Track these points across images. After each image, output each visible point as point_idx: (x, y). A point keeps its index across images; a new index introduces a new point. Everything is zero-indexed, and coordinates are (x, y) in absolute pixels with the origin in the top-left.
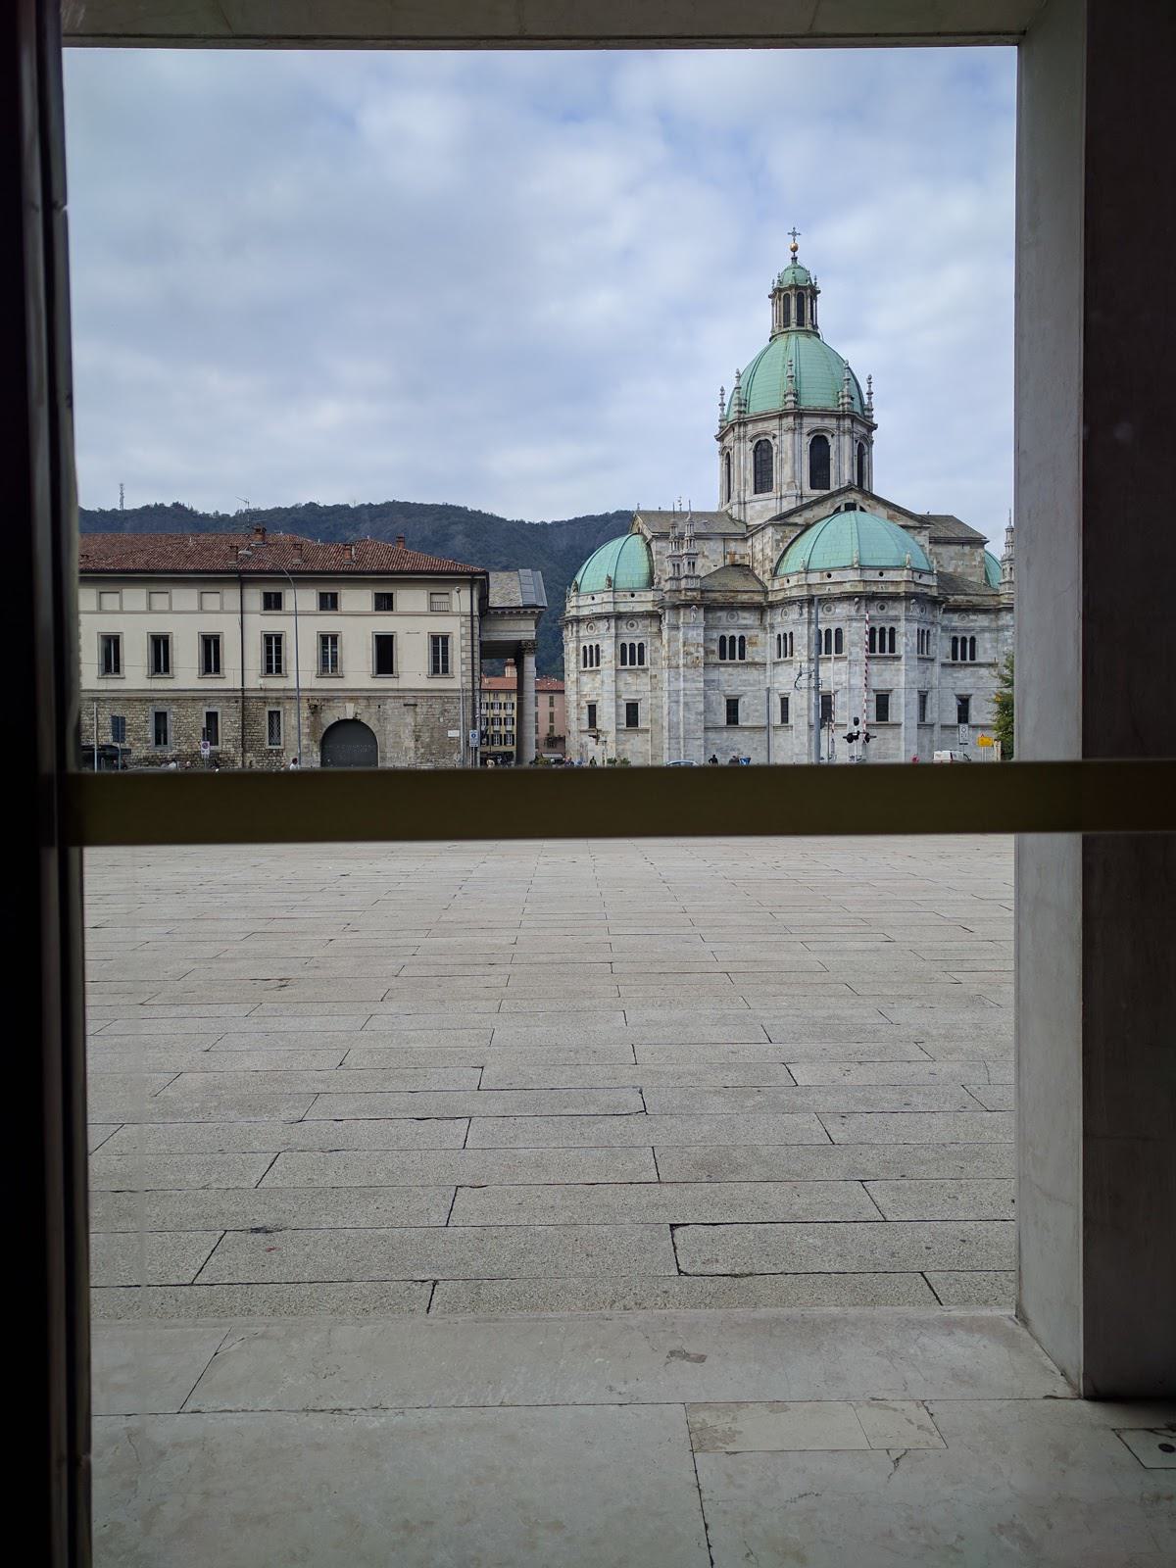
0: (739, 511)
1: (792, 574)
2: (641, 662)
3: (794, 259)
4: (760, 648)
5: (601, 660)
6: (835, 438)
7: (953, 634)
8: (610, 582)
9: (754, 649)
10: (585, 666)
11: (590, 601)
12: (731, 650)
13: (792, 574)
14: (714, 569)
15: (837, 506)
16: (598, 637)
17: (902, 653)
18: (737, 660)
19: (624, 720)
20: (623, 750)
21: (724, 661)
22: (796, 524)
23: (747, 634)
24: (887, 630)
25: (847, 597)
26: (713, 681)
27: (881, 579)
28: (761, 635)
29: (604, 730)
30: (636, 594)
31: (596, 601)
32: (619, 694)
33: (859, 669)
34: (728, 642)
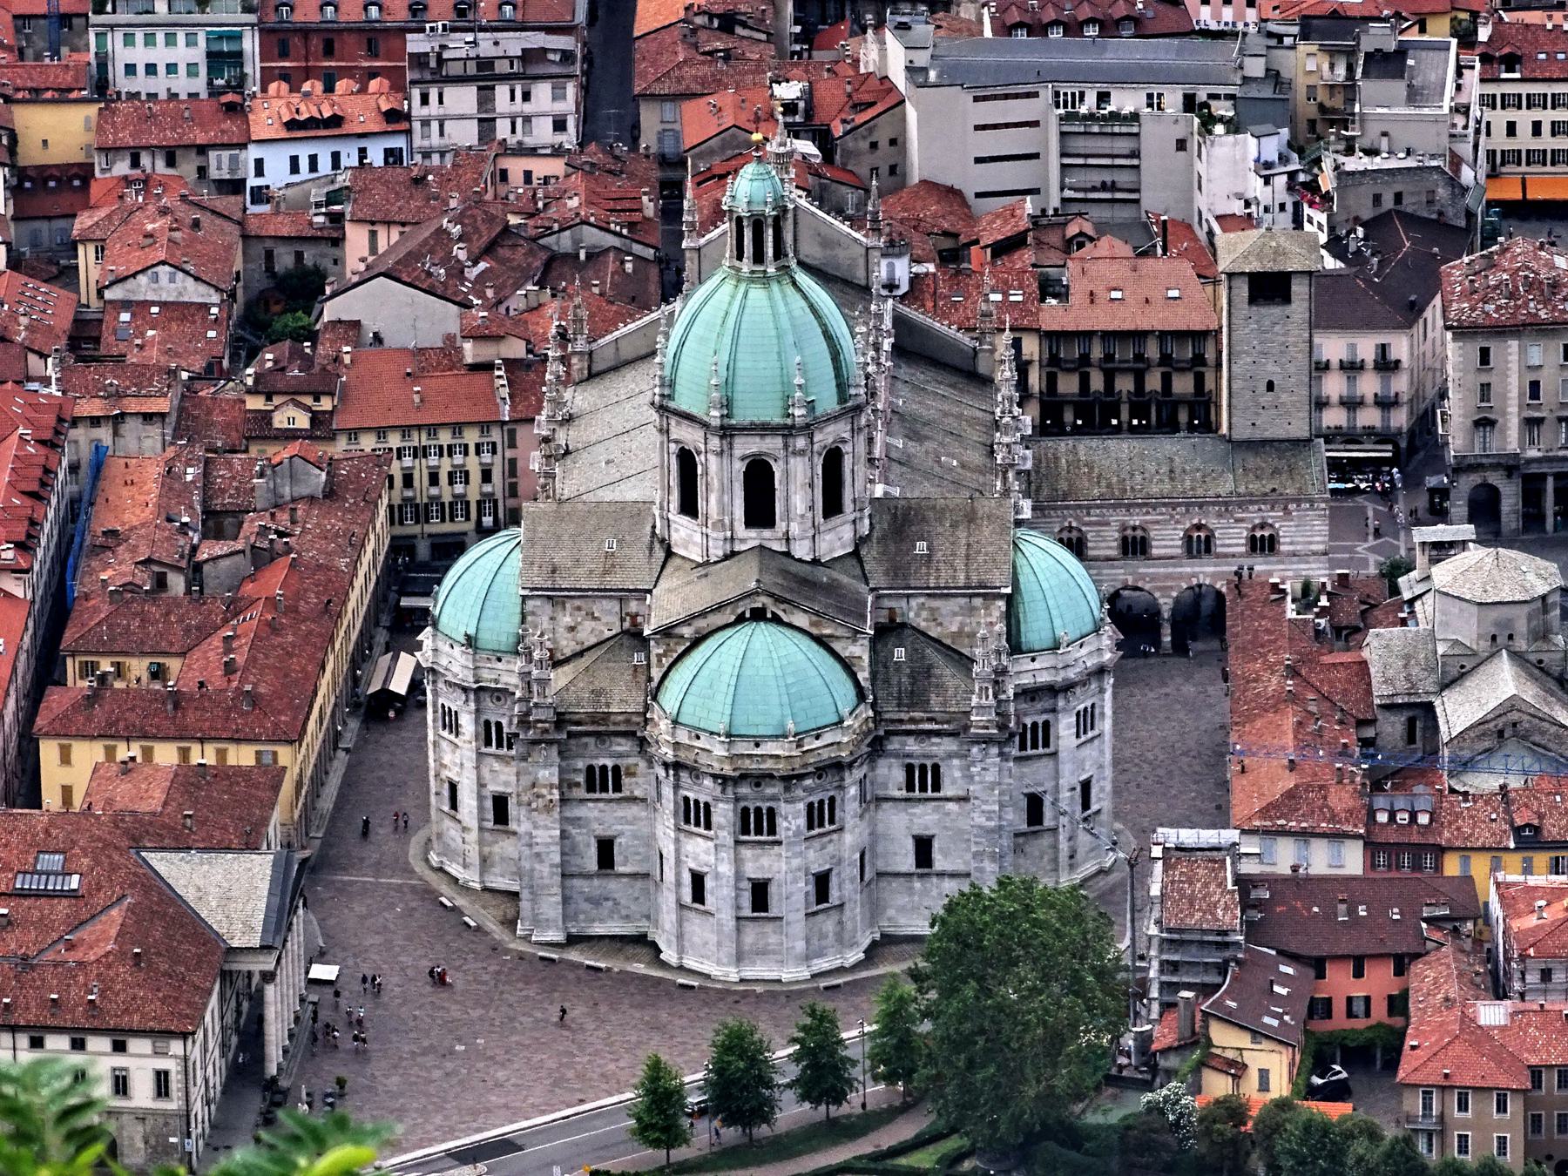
4: (640, 780)
6: (781, 463)
12: (603, 781)
14: (608, 634)
15: (740, 611)
19: (490, 816)
22: (682, 637)
23: (623, 763)
26: (579, 819)
28: (642, 764)
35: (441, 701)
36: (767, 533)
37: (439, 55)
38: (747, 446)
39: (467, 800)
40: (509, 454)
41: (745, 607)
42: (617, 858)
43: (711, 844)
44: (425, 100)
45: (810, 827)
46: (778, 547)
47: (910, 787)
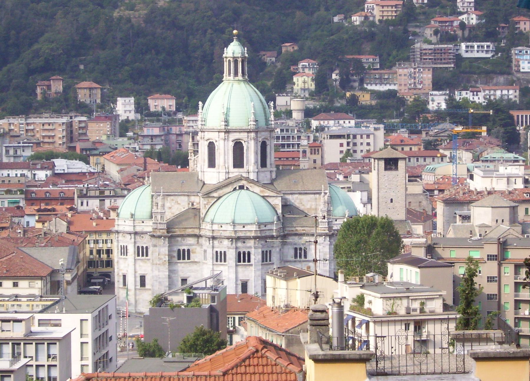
0: (201, 175)
2: (147, 255)
5: (128, 254)
6: (246, 143)
7: (295, 246)
8: (132, 215)
9: (195, 255)
11: (123, 223)
15: (235, 187)
19: (139, 283)
22: (214, 197)
23: (191, 248)
24: (246, 253)
25: (228, 238)
26: (175, 270)
33: (233, 270)
34: (182, 252)
35: (120, 245)
36: (241, 170)
37: (87, 190)
38: (234, 136)
39: (130, 280)
41: (237, 185)
44: (82, 204)
45: (263, 261)
46: (245, 175)
47: (296, 256)
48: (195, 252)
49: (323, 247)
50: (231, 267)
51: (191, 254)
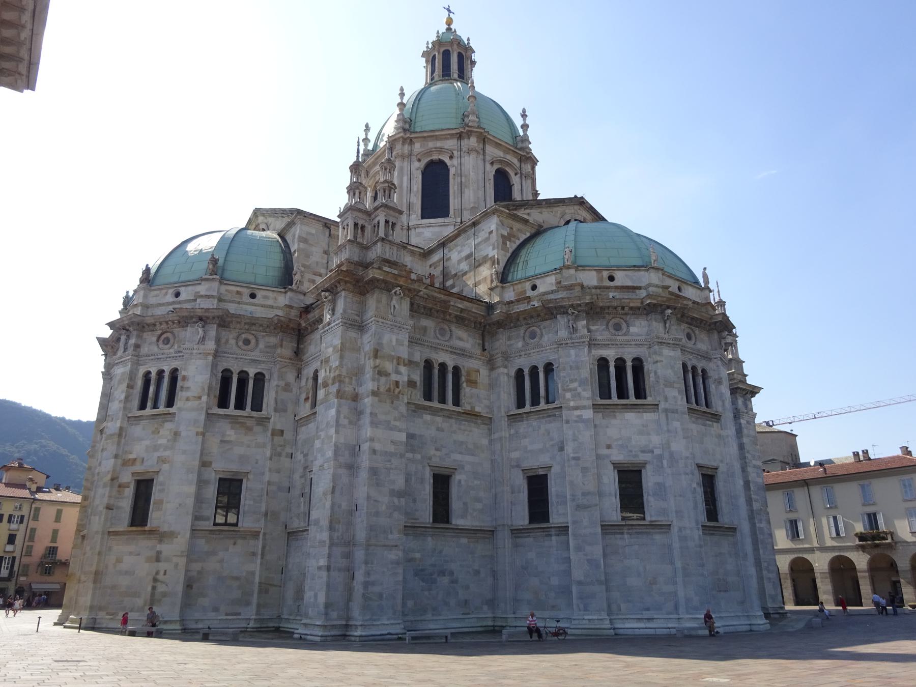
1: (546, 274)
2: (257, 406)
3: (449, 29)
4: (482, 392)
9: (474, 391)
10: (143, 406)
13: (546, 274)
16: (179, 355)
17: (720, 409)
18: (449, 406)
20: (199, 572)
21: (427, 403)
22: (526, 221)
23: (467, 364)
25: (651, 309)
27: (681, 294)
28: (484, 372)
29: (165, 528)
30: (259, 294)
31: (183, 297)
32: (206, 459)
34: (436, 371)
40: (32, 524)
42: (456, 505)
43: (648, 416)
48: (473, 383)
49: (748, 422)
50: (675, 411)
51: (464, 385)
